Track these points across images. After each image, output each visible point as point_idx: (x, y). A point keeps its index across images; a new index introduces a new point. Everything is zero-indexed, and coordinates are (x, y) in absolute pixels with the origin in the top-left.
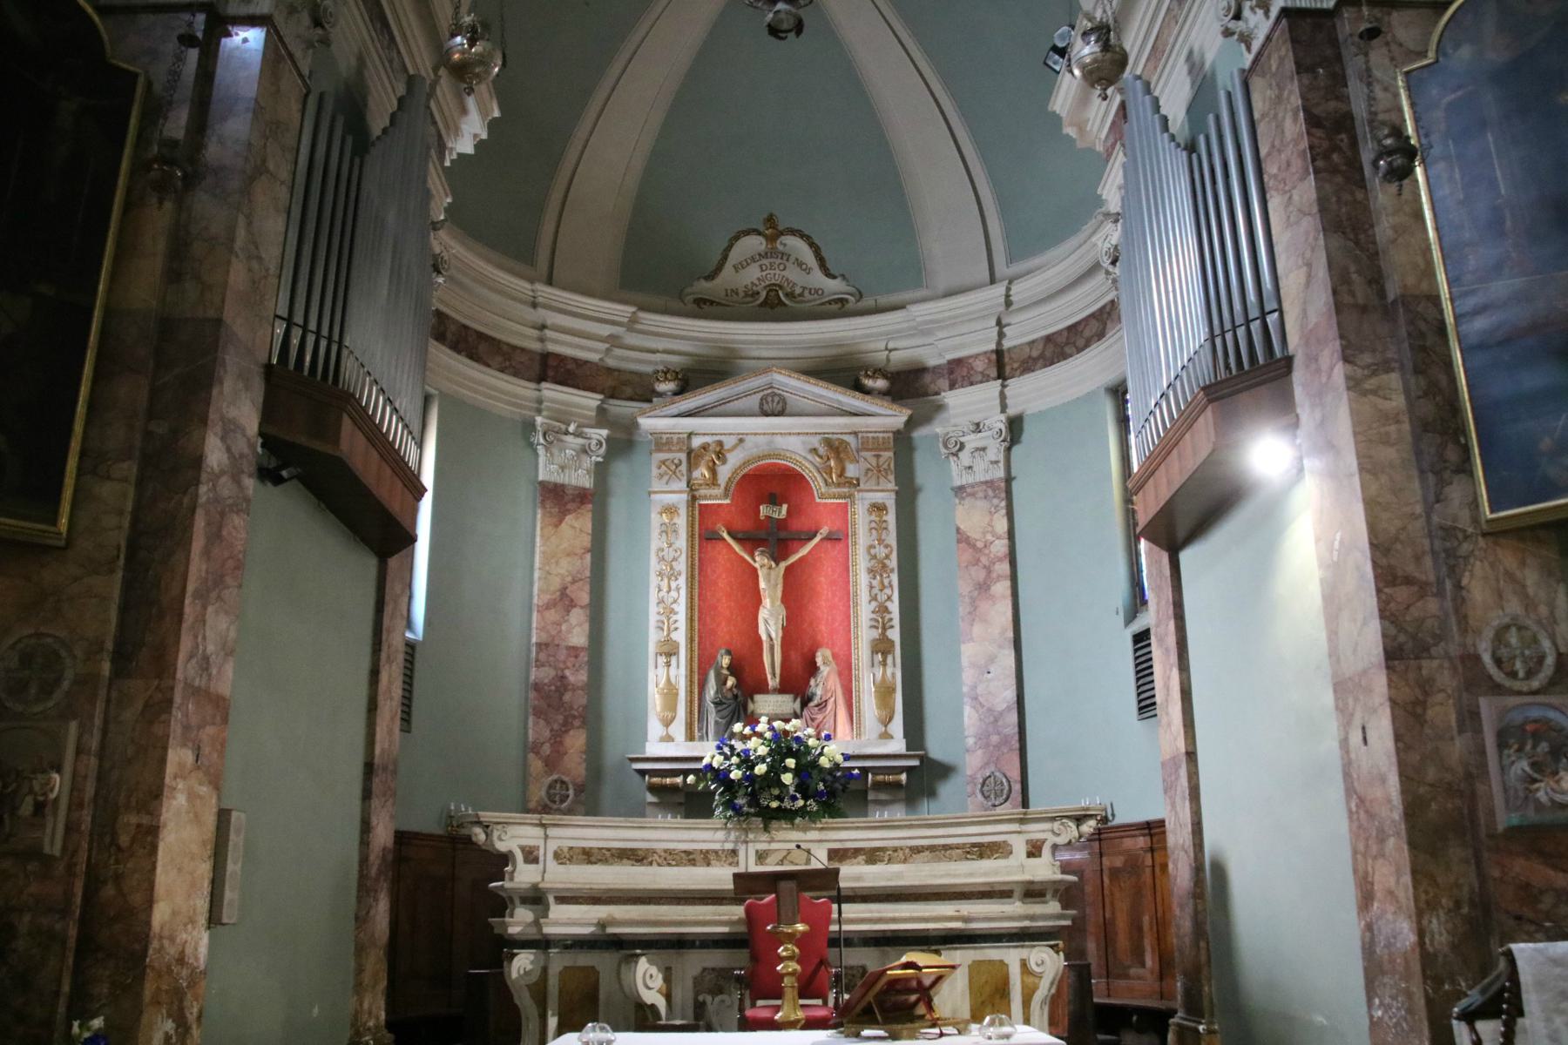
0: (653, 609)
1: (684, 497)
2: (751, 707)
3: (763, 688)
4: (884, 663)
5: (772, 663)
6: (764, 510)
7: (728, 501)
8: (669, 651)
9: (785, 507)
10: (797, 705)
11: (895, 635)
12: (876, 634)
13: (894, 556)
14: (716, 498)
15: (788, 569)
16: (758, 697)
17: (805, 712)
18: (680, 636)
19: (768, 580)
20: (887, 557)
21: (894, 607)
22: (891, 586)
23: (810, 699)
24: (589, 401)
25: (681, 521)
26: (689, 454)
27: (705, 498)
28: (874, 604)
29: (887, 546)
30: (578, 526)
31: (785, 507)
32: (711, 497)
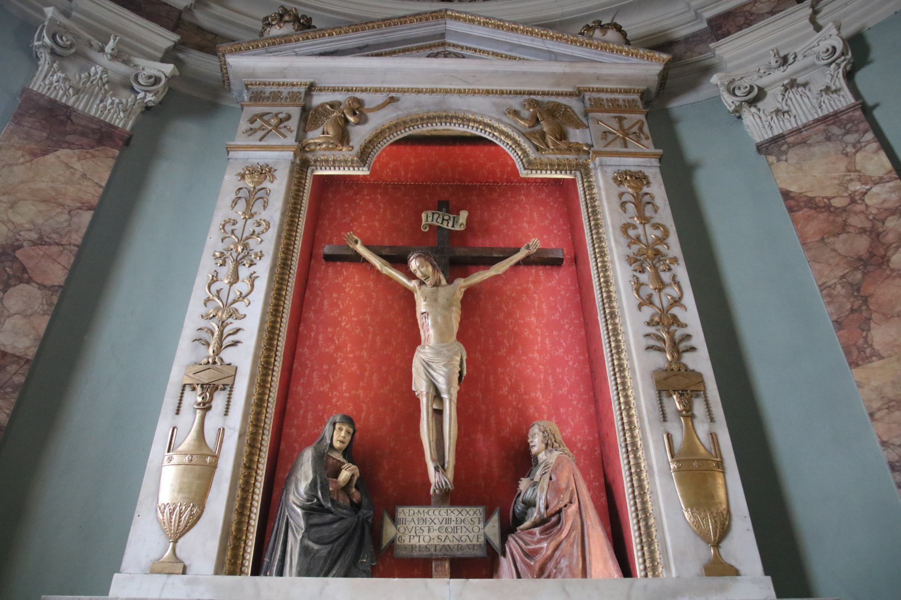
0: (193, 318)
1: (289, 155)
2: (390, 531)
3: (419, 495)
4: (688, 414)
5: (437, 443)
6: (427, 218)
7: (364, 172)
8: (212, 387)
9: (464, 215)
10: (493, 529)
11: (700, 361)
12: (661, 360)
13: (673, 239)
14: (345, 163)
15: (470, 292)
16: (406, 513)
17: (512, 543)
18: (243, 358)
19: (433, 300)
20: (662, 240)
21: (690, 315)
22: (675, 281)
23: (519, 520)
24: (165, 39)
25: (278, 189)
26: (305, 110)
27: (326, 163)
28: (648, 312)
29: (656, 226)
30: (84, 174)
31: (464, 215)
32: (335, 163)
